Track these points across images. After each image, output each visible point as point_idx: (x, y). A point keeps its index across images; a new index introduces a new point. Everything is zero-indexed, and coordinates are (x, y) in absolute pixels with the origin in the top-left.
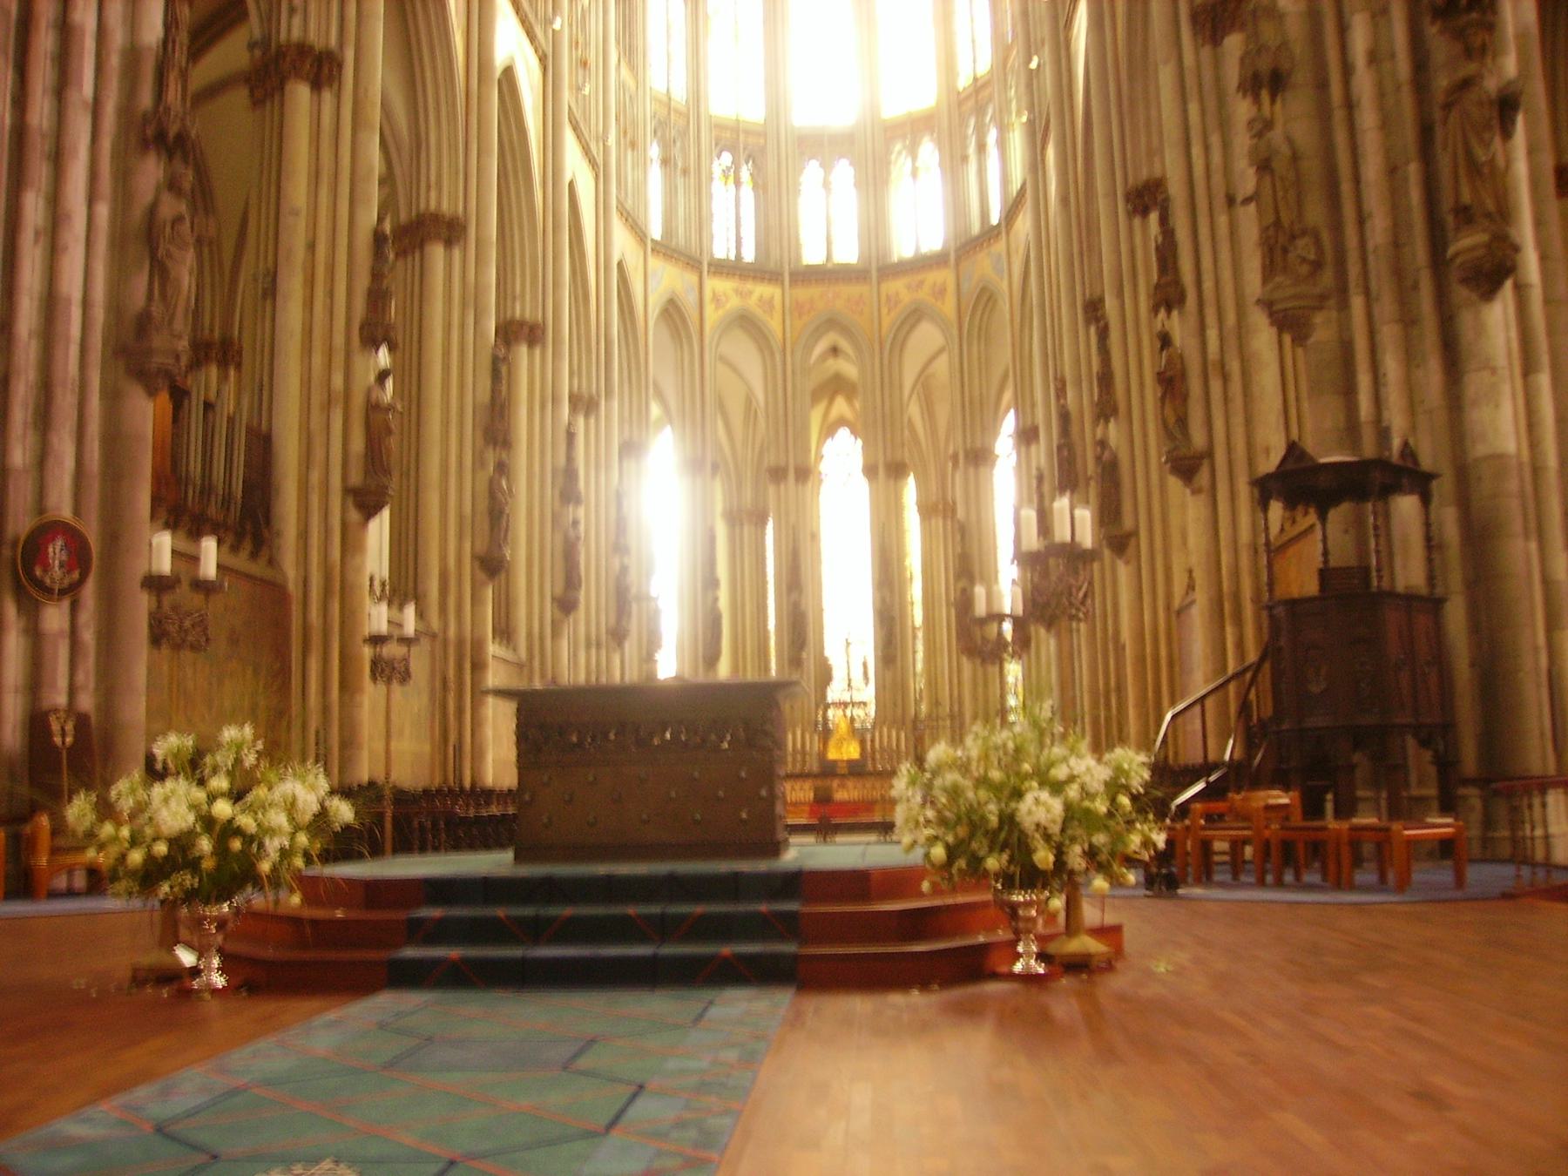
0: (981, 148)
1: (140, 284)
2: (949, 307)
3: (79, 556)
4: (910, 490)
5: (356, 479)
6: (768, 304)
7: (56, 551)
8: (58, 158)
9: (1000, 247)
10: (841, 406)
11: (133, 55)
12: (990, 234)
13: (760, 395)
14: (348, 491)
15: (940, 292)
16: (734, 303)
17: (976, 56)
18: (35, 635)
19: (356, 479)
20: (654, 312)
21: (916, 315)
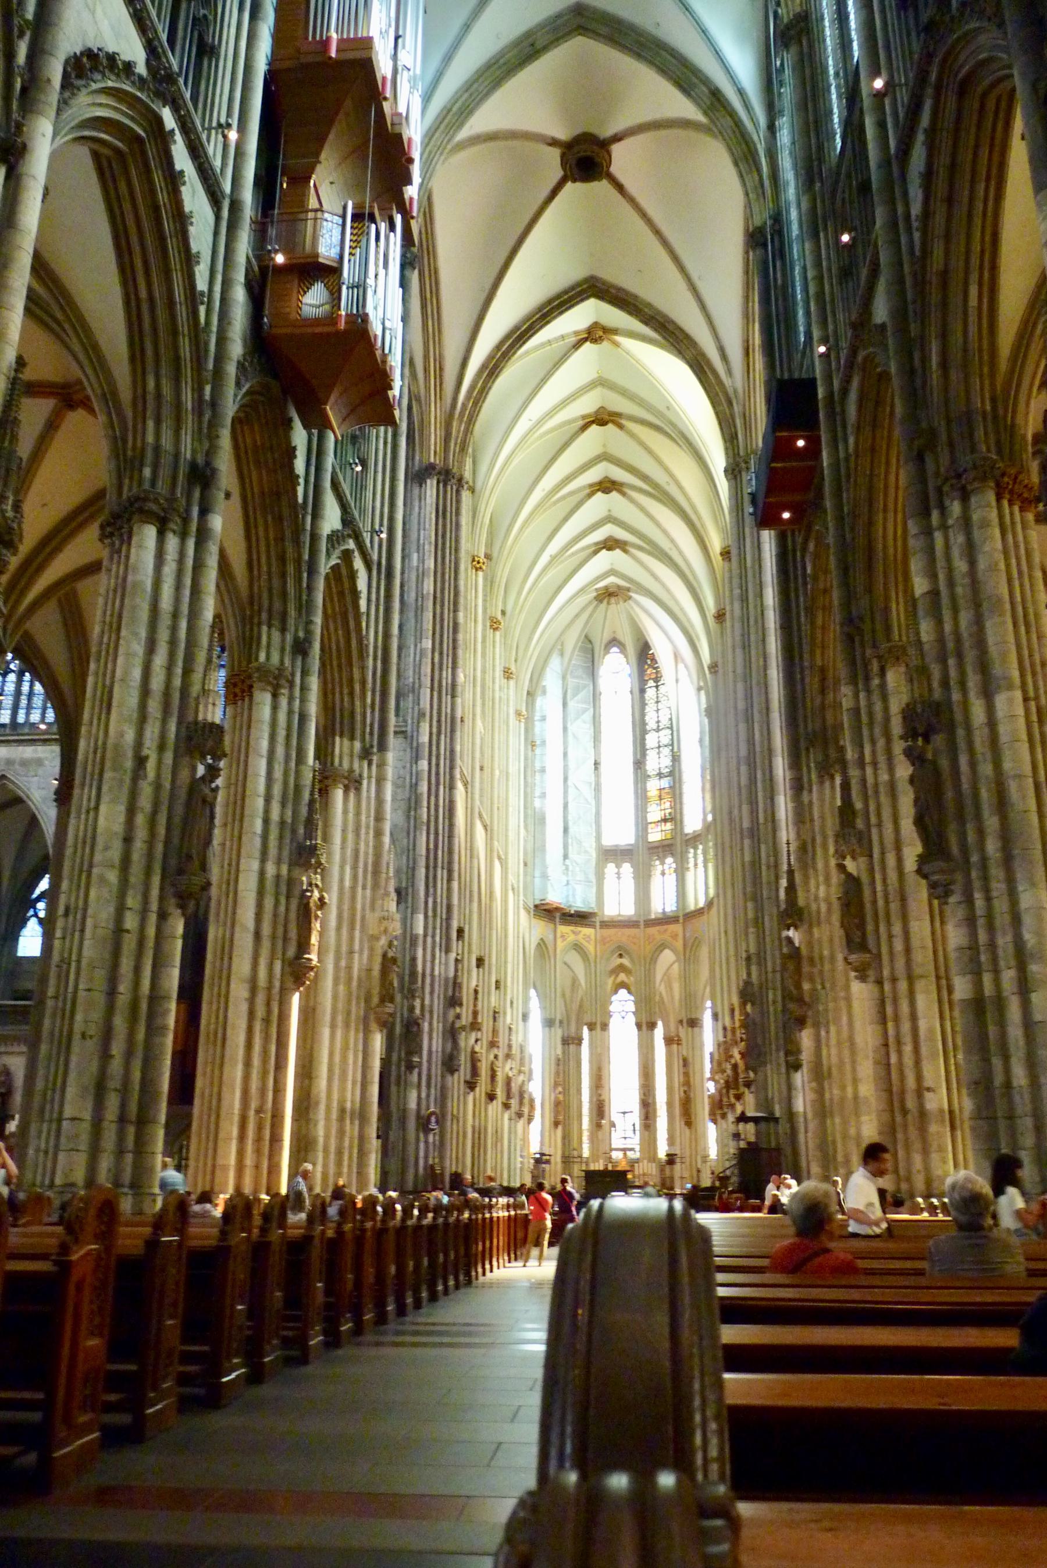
0: (696, 865)
1: (449, 1046)
2: (679, 944)
3: (437, 1122)
4: (659, 1032)
5: (468, 1078)
6: (587, 938)
7: (433, 1119)
8: (431, 1012)
9: (705, 917)
10: (622, 977)
11: (447, 979)
12: (699, 912)
13: (583, 982)
14: (466, 1082)
15: (675, 936)
16: (571, 938)
17: (694, 821)
18: (426, 1142)
19: (468, 1078)
20: (533, 946)
21: (662, 947)
